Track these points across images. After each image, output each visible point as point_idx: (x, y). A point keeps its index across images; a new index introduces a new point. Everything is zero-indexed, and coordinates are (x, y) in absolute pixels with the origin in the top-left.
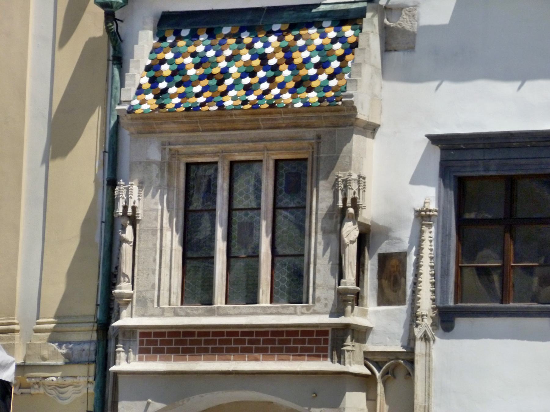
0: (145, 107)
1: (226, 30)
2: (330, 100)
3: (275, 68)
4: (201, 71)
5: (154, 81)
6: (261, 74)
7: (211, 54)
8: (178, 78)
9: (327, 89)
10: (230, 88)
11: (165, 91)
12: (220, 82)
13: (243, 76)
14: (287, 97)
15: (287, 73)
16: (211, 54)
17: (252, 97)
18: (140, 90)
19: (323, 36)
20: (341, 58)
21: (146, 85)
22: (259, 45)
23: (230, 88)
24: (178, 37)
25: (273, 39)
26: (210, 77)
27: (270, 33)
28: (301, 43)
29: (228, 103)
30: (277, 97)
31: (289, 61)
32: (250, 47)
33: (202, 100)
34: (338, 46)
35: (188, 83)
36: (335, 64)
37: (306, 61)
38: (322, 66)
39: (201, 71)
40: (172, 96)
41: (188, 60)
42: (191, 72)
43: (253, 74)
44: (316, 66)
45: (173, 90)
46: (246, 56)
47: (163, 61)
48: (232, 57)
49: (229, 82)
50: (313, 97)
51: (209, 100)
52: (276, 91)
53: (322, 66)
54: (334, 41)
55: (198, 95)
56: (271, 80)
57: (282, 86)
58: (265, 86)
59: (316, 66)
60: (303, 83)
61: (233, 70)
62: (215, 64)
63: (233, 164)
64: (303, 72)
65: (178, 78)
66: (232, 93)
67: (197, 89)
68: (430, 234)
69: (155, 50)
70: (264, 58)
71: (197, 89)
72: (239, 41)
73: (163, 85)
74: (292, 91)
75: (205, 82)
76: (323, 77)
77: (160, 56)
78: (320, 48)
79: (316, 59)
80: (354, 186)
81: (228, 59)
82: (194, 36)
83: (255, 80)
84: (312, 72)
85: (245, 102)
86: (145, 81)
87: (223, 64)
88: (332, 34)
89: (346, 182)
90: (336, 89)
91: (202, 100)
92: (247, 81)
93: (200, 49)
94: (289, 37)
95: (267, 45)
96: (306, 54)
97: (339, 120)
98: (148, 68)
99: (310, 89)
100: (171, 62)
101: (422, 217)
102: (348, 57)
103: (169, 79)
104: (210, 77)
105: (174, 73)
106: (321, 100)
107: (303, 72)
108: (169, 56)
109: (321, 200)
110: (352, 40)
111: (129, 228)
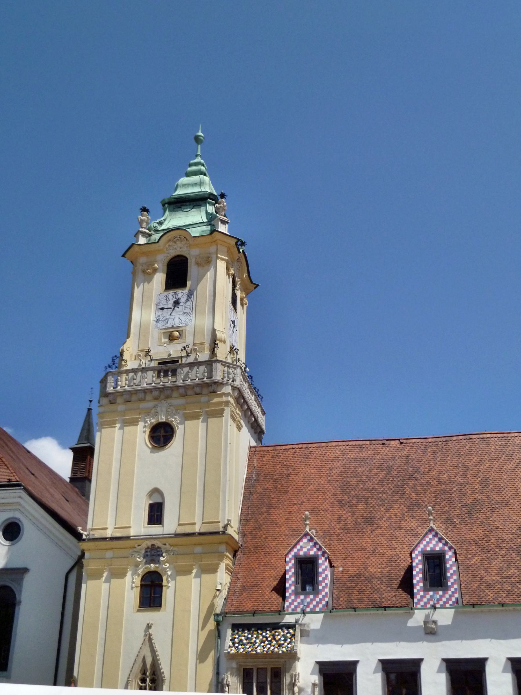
0: (232, 652)
1: (253, 629)
2: (290, 651)
3: (271, 641)
4: (248, 641)
5: (234, 644)
6: (267, 642)
7: (250, 636)
8: (241, 643)
9: (288, 647)
10: (258, 646)
11: (237, 647)
12: (254, 645)
13: (261, 643)
14: (276, 649)
15: (274, 642)
16: (250, 636)
17: (265, 649)
18: (230, 647)
19: (283, 632)
20: (290, 638)
21: (231, 645)
22: (264, 634)
23: (258, 646)
24: (239, 631)
25: (268, 632)
26: (251, 643)
27: (267, 630)
28: (277, 634)
29: (259, 651)
30: (273, 649)
31: (275, 639)
32: (261, 634)
33: (250, 650)
34: (288, 635)
35: (244, 644)
36: (289, 640)
37: (280, 639)
38: (285, 640)
39: (248, 641)
40: (240, 649)
41: (243, 638)
42: (245, 641)
43: (264, 643)
44: (283, 641)
45: (240, 647)
46: (261, 637)
47: (235, 638)
48: (257, 638)
49: (257, 645)
50: (284, 649)
51: (252, 650)
52: (272, 648)
53: (285, 640)
54: (287, 633)
55: (248, 648)
56: (270, 644)
57: (274, 646)
58: (269, 646)
59: (283, 641)
60: (280, 645)
61: (258, 641)
62: (252, 639)
63: (258, 669)
64: (279, 642)
65: (241, 643)
66: (259, 648)
67: (248, 646)
68: (317, 690)
69: (233, 634)
70: (267, 638)
71: (248, 646)
72: (258, 633)
73: (237, 645)
74: (277, 648)
75: (250, 645)
76: (286, 644)
77: (234, 636)
78: (283, 636)
79: (283, 639)
80: (297, 676)
81: (255, 638)
82: (243, 631)
83: (265, 644)
84: (282, 642)
85: (264, 651)
86: (231, 644)
87: (254, 639)
88: (286, 631)
89: (295, 675)
90: (290, 648)
91: (250, 650)
92: (262, 644)
93: (246, 635)
94: (273, 632)
95: (267, 634)
96: (279, 637)
97: (292, 656)
98: (231, 640)
99: (283, 648)
100: (238, 638)
101: (314, 685)
102: (293, 638)
103: (238, 643)
104: (251, 643)
105: (239, 642)
106: (287, 651)
107: (279, 642)
108: (237, 636)
109: (287, 680)
110: (293, 633)
111: (227, 688)
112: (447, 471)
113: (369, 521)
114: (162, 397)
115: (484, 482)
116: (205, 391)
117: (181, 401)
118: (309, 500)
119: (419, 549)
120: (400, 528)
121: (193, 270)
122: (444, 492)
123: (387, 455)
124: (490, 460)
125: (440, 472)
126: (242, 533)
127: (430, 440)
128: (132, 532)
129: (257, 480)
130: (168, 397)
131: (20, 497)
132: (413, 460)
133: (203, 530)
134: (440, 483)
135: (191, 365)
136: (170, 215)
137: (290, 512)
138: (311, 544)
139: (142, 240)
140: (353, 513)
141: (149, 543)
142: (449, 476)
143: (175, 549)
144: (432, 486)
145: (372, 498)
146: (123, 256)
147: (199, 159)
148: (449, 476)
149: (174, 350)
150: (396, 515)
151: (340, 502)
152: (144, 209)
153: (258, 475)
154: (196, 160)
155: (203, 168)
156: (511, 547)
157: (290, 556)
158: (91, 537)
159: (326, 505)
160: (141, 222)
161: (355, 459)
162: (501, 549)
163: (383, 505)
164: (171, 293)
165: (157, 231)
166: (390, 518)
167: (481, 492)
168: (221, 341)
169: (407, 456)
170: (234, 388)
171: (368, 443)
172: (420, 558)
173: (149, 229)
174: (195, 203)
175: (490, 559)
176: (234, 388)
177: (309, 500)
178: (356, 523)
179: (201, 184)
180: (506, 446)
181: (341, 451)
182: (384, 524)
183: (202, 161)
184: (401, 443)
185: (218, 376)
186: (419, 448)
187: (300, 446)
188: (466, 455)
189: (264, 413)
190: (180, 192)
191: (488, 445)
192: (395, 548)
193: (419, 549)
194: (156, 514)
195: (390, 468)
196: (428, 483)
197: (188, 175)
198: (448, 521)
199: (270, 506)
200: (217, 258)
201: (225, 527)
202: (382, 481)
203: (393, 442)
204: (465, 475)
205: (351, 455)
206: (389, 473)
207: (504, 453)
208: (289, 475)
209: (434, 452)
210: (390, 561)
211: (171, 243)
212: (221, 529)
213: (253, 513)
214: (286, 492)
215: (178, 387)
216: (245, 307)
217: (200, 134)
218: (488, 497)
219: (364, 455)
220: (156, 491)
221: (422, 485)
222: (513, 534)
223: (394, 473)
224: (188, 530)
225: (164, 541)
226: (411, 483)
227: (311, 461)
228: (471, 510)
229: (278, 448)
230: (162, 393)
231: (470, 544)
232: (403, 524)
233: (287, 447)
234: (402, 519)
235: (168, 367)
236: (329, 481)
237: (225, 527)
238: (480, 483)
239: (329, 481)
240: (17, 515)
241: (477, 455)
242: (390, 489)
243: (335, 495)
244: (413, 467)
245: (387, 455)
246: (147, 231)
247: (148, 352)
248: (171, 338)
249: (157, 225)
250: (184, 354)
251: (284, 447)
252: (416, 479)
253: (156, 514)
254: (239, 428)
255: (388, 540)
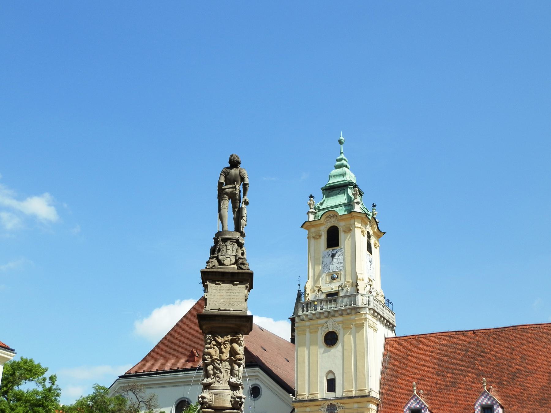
112: (501, 351)
113: (454, 384)
114: (330, 316)
115: (523, 358)
116: (353, 312)
117: (340, 319)
118: (419, 371)
119: (478, 403)
120: (472, 388)
121: (342, 235)
122: (498, 364)
123: (466, 341)
124: (528, 343)
125: (497, 352)
126: (381, 393)
127: (492, 330)
128: (319, 397)
129: (390, 360)
130: (333, 316)
131: (259, 372)
132: (481, 344)
133: (357, 395)
134: (497, 359)
135: (345, 296)
136: (327, 199)
137: (408, 380)
138: (418, 401)
139: (312, 217)
140: (445, 379)
141: (329, 403)
142: (502, 354)
143: (343, 405)
144: (492, 361)
145: (456, 369)
146: (302, 227)
147: (342, 156)
148: (502, 354)
149: (334, 287)
150: (469, 380)
151: (437, 372)
152: (311, 197)
153: (390, 356)
154: (340, 157)
155: (344, 162)
156: (536, 399)
157: (406, 408)
158: (297, 400)
159: (429, 375)
160: (310, 204)
161: (447, 345)
162: (530, 401)
163: (462, 374)
164: (330, 249)
165: (320, 210)
166: (466, 382)
167: (521, 365)
168: (360, 280)
169: (478, 342)
170: (370, 309)
171: (454, 333)
172: (479, 408)
173: (315, 209)
174: (341, 189)
175: (523, 407)
176: (370, 309)
177: (419, 371)
178: (447, 386)
179: (343, 175)
180: (538, 333)
181: (438, 339)
182: (462, 386)
183: (344, 158)
184: (474, 333)
185: (359, 304)
186: (485, 336)
187: (414, 337)
188: (513, 340)
189: (394, 314)
190: (333, 181)
191: (527, 332)
192: (468, 401)
193: (478, 403)
194: (331, 385)
195: (467, 350)
196: (489, 359)
197: (337, 167)
198: (500, 384)
199: (397, 376)
200: (355, 227)
201: (369, 392)
202: (462, 358)
203: (469, 333)
204: (511, 354)
205: (445, 342)
206: (466, 353)
207: (536, 338)
208: (408, 356)
209: (494, 338)
210: (465, 409)
211: (328, 219)
212: (367, 394)
213: (388, 381)
214: (406, 367)
215: (337, 311)
216: (378, 248)
217: (342, 138)
218: (524, 367)
219: (452, 341)
220: (331, 372)
221: (485, 360)
222: (538, 391)
223: (469, 353)
224: (350, 395)
225: (337, 401)
226: (479, 359)
227: (421, 347)
228: (514, 376)
229: (402, 338)
230: (329, 315)
231: (512, 398)
232: (474, 385)
233: (406, 338)
234: (473, 383)
235: (332, 296)
236: (431, 359)
237: (369, 392)
238: (521, 358)
239: (431, 359)
240: (257, 382)
241: (520, 340)
242: (466, 363)
243: (434, 368)
244: (481, 349)
245: (466, 341)
246: (314, 211)
247: (319, 290)
248: (333, 279)
249: (319, 205)
250: (340, 289)
251: (405, 338)
252: (482, 356)
253: (331, 385)
254: (375, 330)
255: (465, 396)
